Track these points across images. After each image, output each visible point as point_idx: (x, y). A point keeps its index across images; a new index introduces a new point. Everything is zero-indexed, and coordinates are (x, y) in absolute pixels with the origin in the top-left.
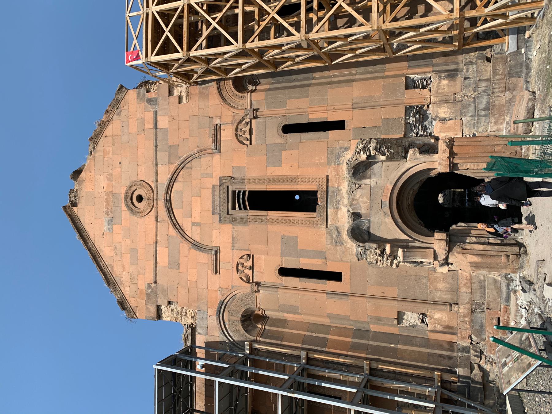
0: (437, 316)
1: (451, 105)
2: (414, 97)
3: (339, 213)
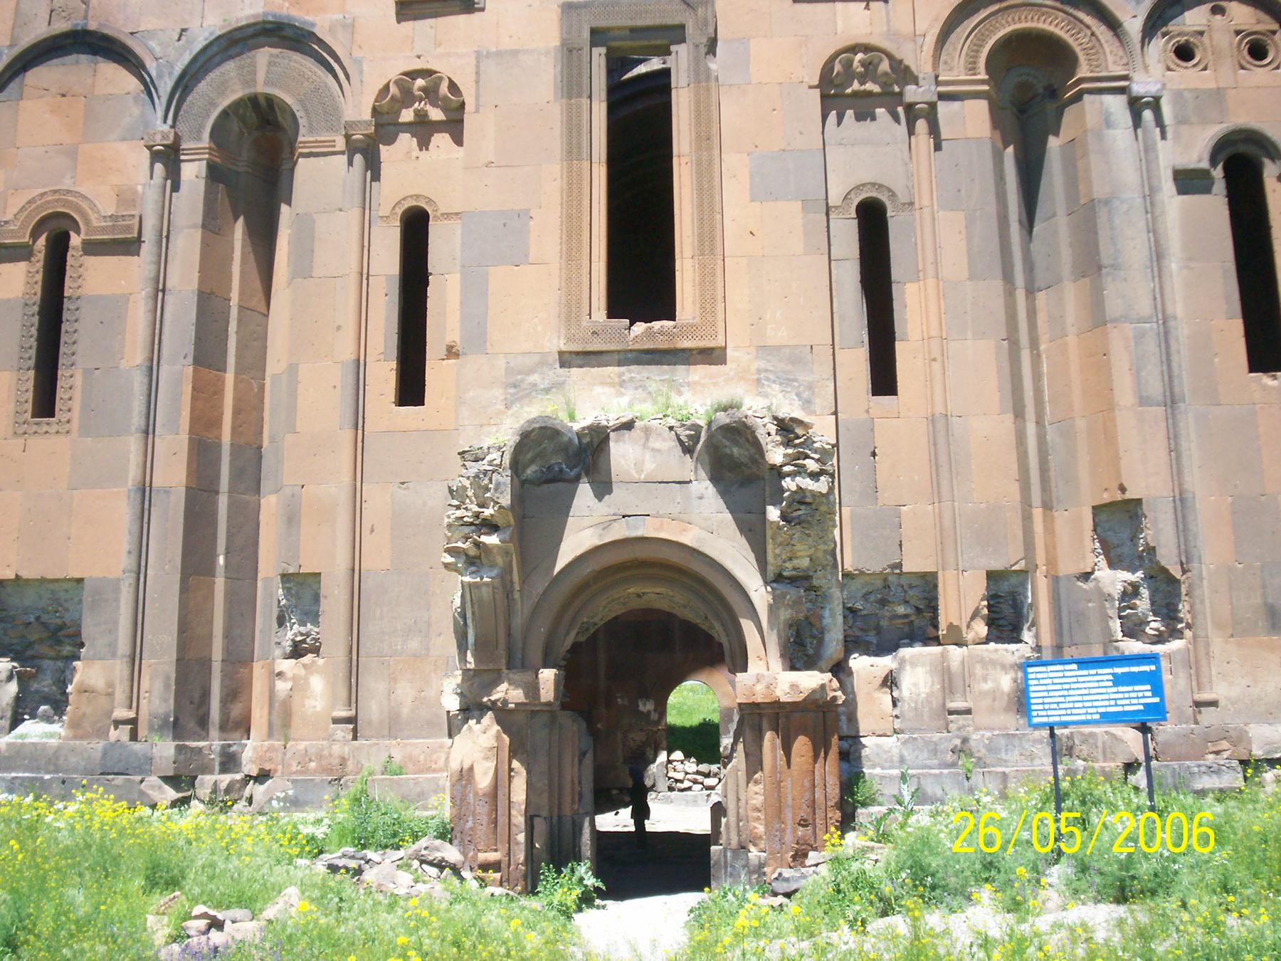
0: (317, 684)
1: (935, 704)
2: (961, 599)
3: (607, 390)
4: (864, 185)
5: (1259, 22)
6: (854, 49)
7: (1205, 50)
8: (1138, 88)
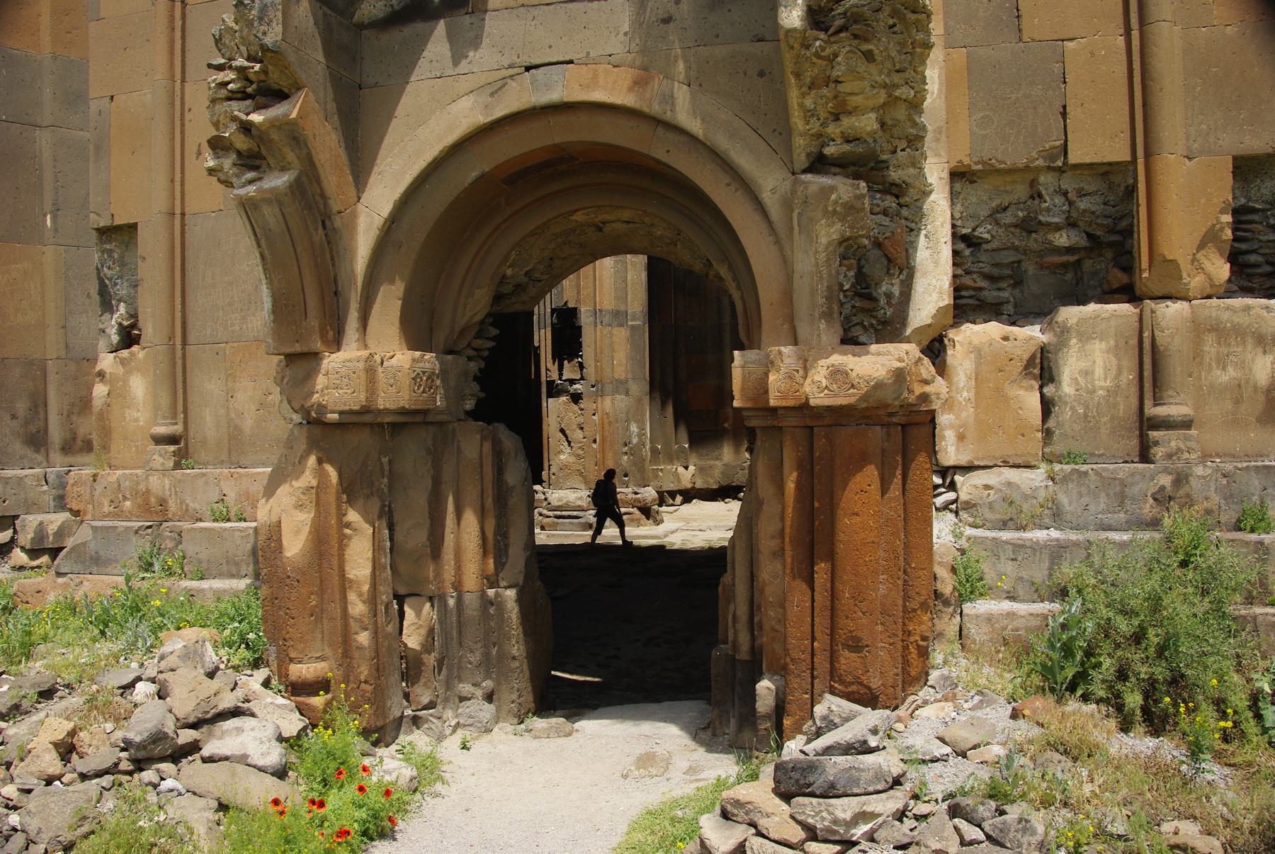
1: (1126, 406)
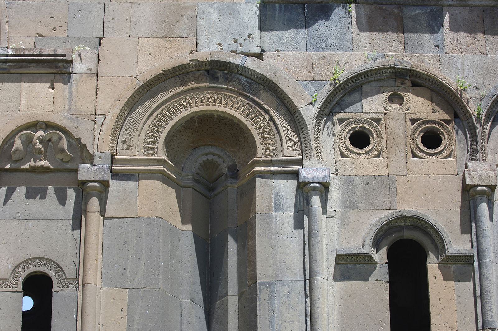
4: (33, 259)
5: (434, 111)
6: (34, 126)
7: (379, 137)
8: (305, 174)
